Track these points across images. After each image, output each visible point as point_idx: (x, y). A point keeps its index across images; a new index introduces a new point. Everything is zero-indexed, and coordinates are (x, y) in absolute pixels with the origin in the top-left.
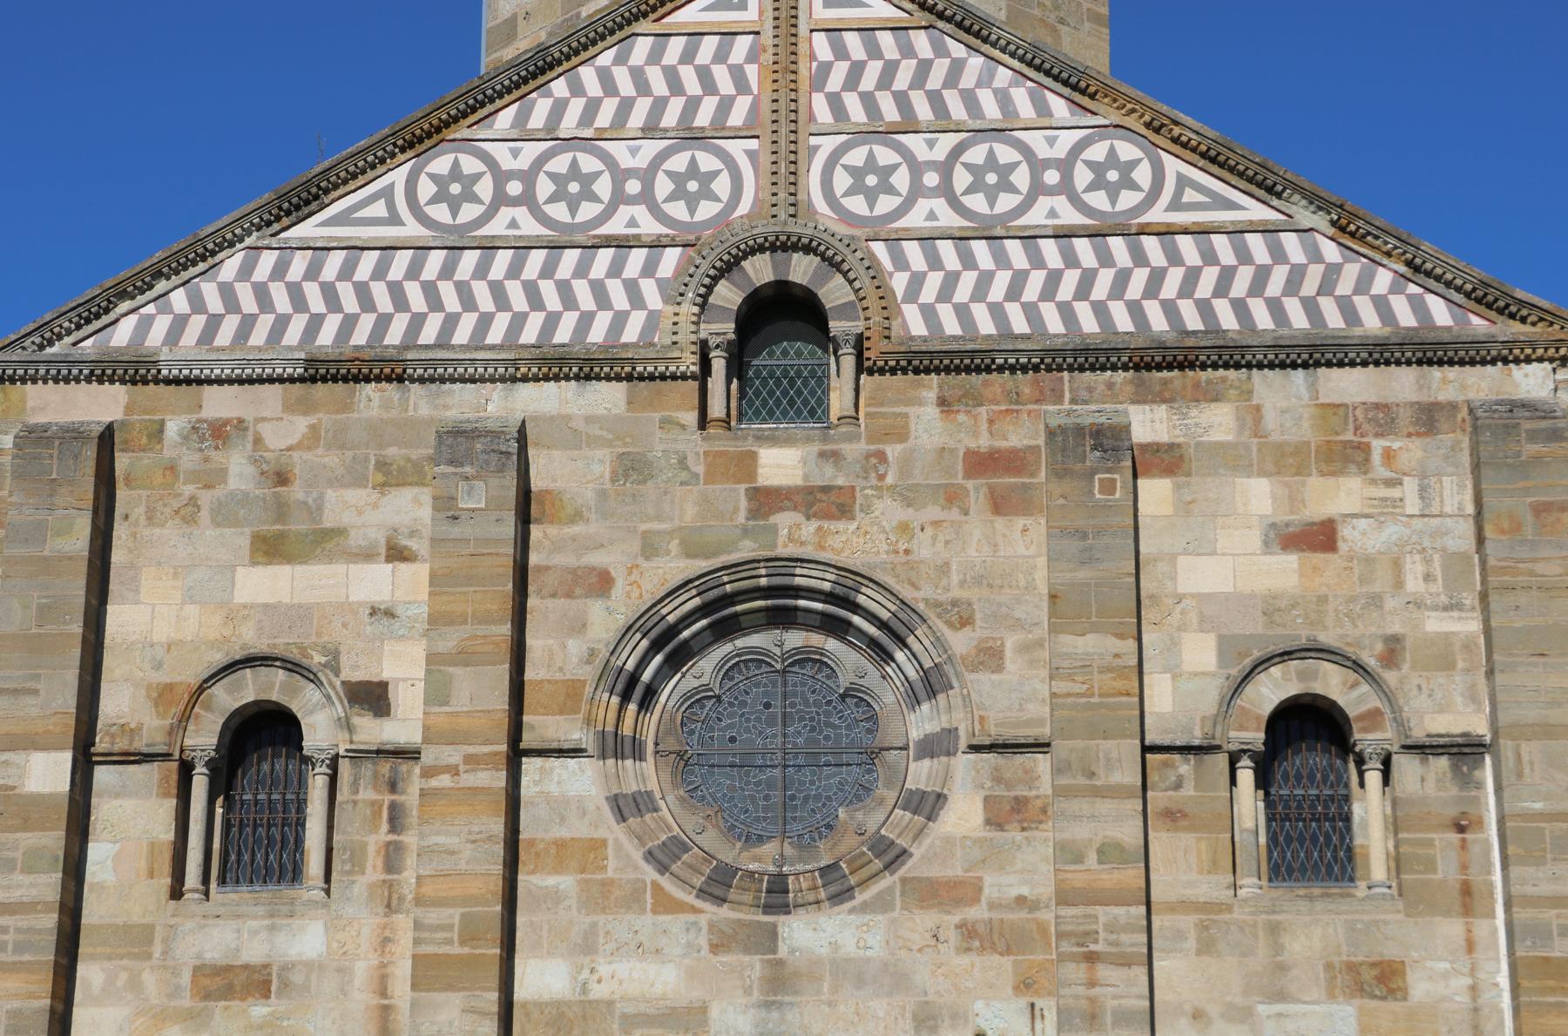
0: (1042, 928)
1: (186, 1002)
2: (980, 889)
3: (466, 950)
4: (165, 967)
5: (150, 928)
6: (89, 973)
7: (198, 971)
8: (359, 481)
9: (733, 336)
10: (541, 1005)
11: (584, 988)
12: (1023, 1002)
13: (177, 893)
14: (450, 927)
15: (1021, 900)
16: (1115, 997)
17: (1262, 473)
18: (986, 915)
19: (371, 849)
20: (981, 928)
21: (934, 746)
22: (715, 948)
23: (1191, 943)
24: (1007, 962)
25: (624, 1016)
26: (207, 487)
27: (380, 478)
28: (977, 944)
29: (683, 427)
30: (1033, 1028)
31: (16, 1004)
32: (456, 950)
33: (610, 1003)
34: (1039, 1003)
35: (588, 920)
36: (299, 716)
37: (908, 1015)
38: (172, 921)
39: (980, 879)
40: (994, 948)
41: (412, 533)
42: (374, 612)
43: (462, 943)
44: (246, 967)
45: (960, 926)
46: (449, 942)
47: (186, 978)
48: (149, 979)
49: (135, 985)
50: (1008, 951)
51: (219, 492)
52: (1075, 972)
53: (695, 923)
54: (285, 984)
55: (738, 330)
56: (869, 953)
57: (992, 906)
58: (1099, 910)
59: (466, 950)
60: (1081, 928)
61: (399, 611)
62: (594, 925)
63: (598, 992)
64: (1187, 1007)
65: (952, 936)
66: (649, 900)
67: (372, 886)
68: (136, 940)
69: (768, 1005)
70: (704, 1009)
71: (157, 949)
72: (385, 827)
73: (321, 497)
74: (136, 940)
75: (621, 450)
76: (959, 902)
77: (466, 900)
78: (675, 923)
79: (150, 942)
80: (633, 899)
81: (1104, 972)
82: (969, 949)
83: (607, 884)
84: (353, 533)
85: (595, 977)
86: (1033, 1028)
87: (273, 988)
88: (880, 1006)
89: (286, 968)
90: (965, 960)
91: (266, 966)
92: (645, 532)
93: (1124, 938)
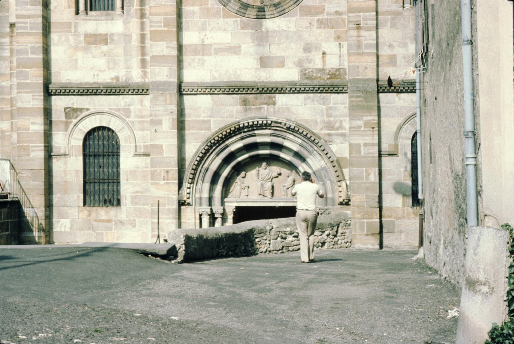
0: (343, 20)
1: (83, 45)
2: (324, 9)
3: (166, 29)
4: (76, 35)
5: (70, 23)
6: (54, 37)
7: (86, 35)
10: (190, 46)
11: (203, 41)
12: (337, 43)
13: (77, 13)
14: (161, 22)
15: (337, 13)
16: (365, 40)
18: (326, 17)
20: (324, 21)
22: (242, 28)
23: (389, 24)
24: (332, 31)
25: (215, 49)
28: (323, 26)
30: (340, 51)
31: (33, 45)
32: (163, 29)
33: (211, 45)
34: (342, 43)
35: (203, 20)
37: (302, 47)
38: (76, 21)
39: (325, 6)
40: (328, 27)
43: (165, 26)
44: (100, 35)
45: (318, 20)
46: (161, 26)
47: (82, 38)
48: (71, 38)
49: (67, 40)
50: (332, 28)
52: (353, 33)
53: (236, 21)
54: (112, 40)
56: (290, 29)
57: (328, 14)
58: (362, 14)
59: (166, 29)
60: (356, 20)
62: (205, 22)
63: (207, 42)
64: (387, 43)
65: (315, 24)
66: (222, 14)
67: (136, 10)
68: (66, 26)
69: (259, 45)
70: (240, 47)
71: (73, 30)
74: (66, 26)
76: (317, 14)
77: (166, 14)
78: (230, 21)
79: (71, 27)
80: (216, 14)
81: (363, 33)
82: (320, 28)
83: (208, 9)
85: (206, 37)
86: (340, 51)
87: (109, 41)
88: (293, 45)
89: (112, 34)
90: (319, 31)
91: (106, 34)
93: (369, 22)
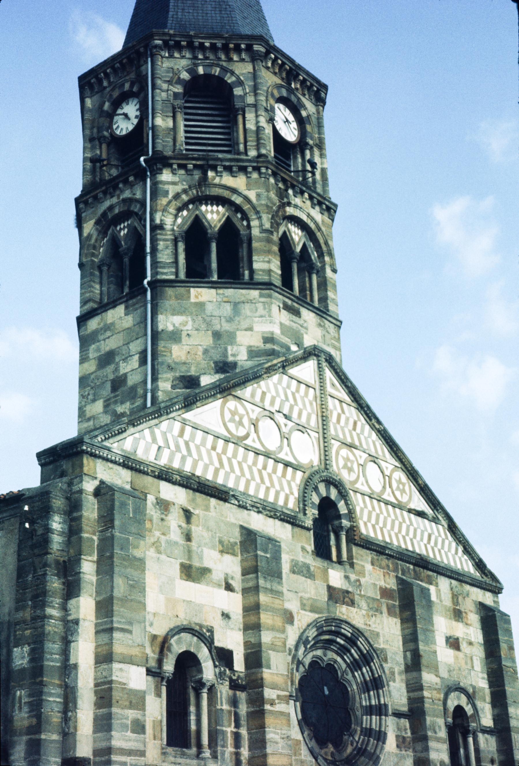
8: (213, 547)
9: (317, 516)
17: (442, 616)
19: (229, 735)
21: (370, 710)
26: (163, 534)
27: (221, 548)
29: (308, 552)
36: (201, 661)
41: (232, 578)
42: (223, 614)
51: (167, 537)
55: (319, 514)
61: (231, 616)
67: (231, 753)
72: (233, 724)
73: (202, 551)
75: (292, 558)
84: (214, 572)
92: (301, 597)
